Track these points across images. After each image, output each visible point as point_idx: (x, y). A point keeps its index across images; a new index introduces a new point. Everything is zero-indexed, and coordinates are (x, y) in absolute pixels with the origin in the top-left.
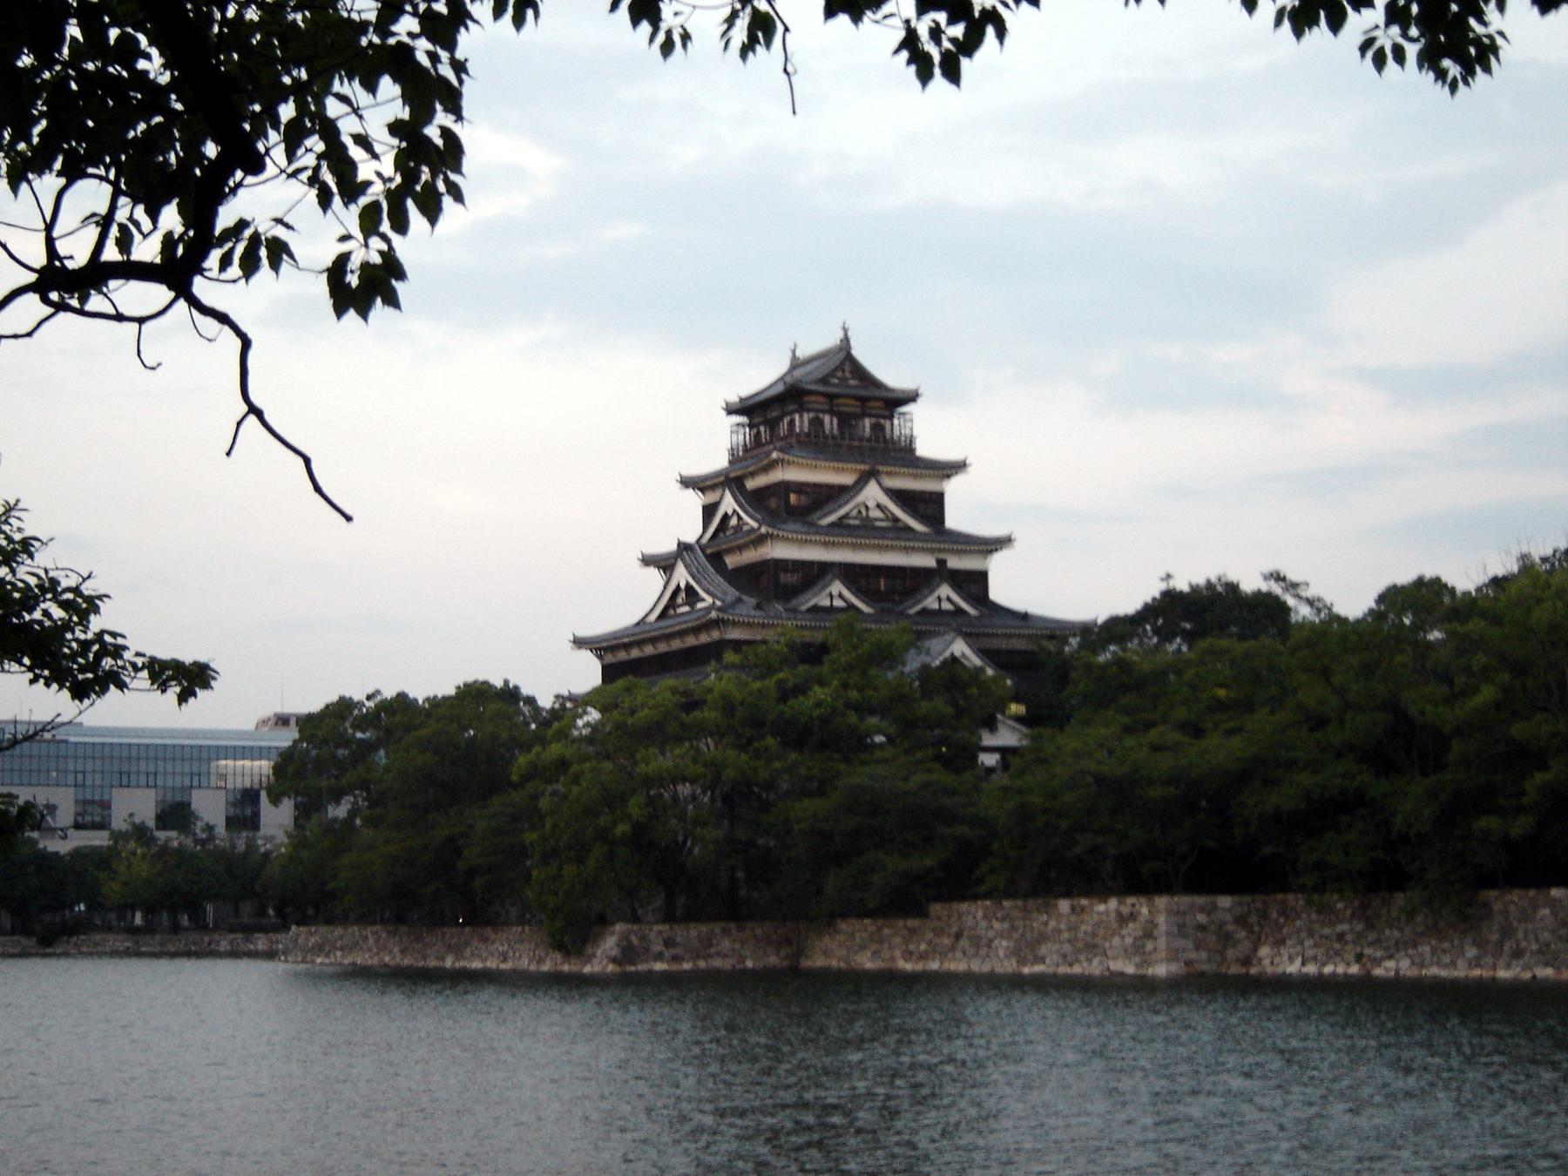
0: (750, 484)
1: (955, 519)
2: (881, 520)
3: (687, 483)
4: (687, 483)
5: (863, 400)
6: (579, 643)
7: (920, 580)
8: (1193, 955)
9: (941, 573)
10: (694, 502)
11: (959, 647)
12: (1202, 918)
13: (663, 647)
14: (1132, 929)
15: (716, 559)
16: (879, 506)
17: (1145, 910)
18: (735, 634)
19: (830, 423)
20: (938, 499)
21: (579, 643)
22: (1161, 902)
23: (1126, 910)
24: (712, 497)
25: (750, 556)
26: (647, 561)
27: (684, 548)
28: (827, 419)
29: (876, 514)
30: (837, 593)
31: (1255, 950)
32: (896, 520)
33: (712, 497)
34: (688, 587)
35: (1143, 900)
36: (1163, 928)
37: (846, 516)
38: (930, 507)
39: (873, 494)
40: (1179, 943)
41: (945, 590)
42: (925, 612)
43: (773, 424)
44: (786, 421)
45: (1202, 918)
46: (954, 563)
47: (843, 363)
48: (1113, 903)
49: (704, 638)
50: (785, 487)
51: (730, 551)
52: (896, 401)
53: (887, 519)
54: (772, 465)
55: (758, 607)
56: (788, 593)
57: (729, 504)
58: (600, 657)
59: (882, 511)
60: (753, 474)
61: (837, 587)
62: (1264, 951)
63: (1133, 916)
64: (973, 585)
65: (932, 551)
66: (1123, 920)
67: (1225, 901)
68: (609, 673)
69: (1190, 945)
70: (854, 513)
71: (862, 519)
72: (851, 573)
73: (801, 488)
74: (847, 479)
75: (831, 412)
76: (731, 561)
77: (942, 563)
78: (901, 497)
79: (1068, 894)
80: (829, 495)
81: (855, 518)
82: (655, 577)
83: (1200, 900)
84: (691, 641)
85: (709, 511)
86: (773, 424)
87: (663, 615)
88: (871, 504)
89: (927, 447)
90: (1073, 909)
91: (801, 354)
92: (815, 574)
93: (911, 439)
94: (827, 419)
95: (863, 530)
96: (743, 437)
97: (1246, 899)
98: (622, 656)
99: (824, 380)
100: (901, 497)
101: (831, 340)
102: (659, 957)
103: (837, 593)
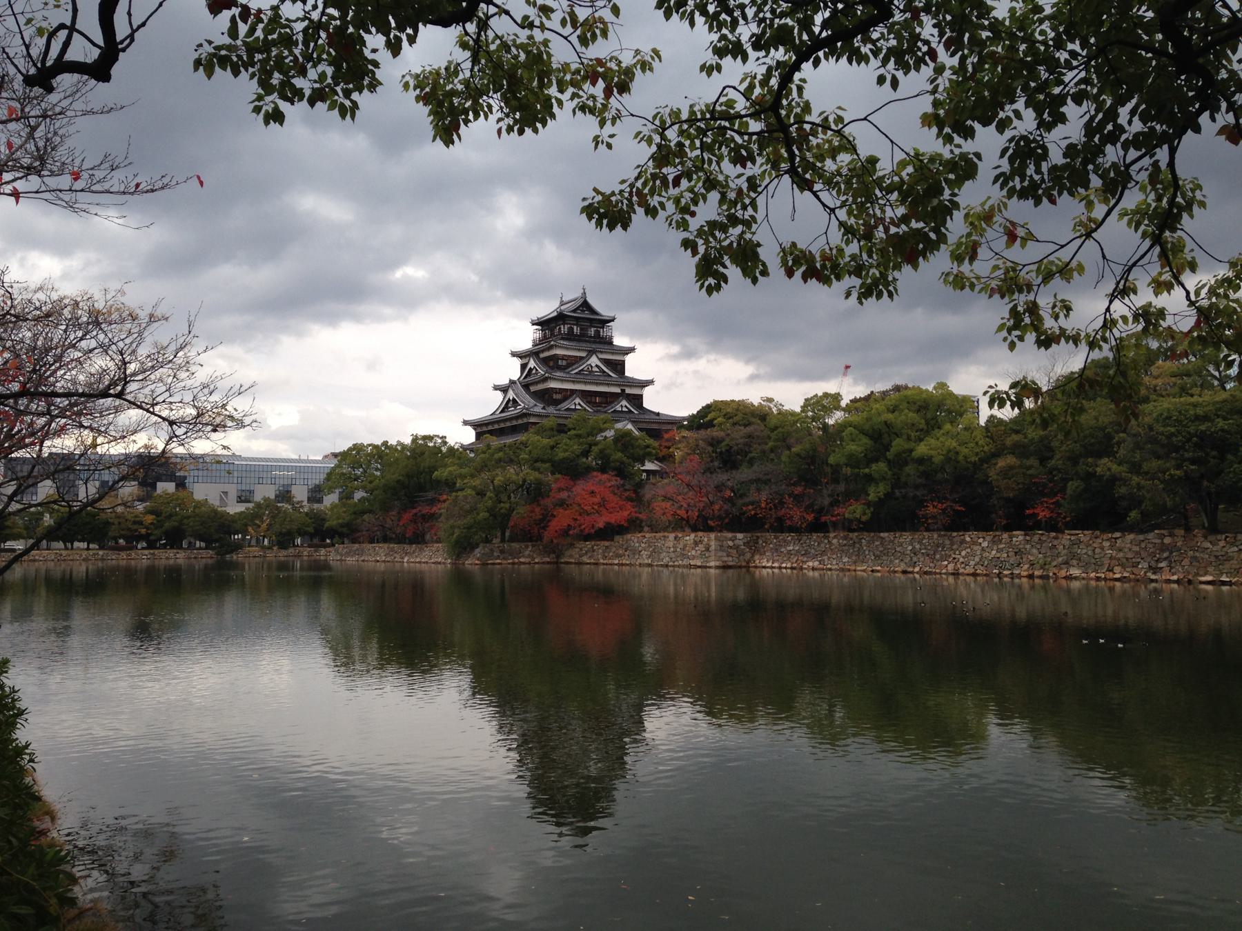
0: (542, 355)
1: (629, 373)
3: (514, 354)
4: (514, 354)
5: (591, 320)
6: (466, 423)
7: (614, 397)
8: (726, 559)
9: (623, 395)
10: (517, 362)
11: (630, 426)
12: (731, 543)
13: (502, 425)
14: (701, 547)
15: (526, 387)
16: (597, 366)
17: (706, 539)
18: (532, 420)
19: (576, 330)
20: (624, 362)
21: (466, 423)
22: (712, 536)
23: (698, 539)
24: (525, 361)
25: (541, 387)
26: (496, 388)
27: (512, 382)
31: (753, 556)
32: (604, 372)
33: (525, 361)
34: (514, 399)
35: (705, 534)
36: (713, 548)
37: (582, 370)
38: (619, 367)
39: (594, 361)
40: (720, 554)
41: (624, 403)
42: (615, 411)
43: (552, 331)
45: (731, 543)
46: (628, 391)
48: (693, 536)
49: (520, 422)
50: (555, 358)
51: (532, 384)
52: (604, 322)
54: (551, 348)
55: (544, 408)
56: (556, 403)
57: (532, 364)
58: (475, 429)
60: (543, 351)
61: (578, 401)
62: (757, 557)
63: (701, 542)
64: (637, 400)
65: (619, 385)
66: (696, 543)
67: (740, 536)
68: (478, 436)
69: (725, 554)
72: (585, 395)
73: (563, 357)
74: (583, 354)
75: (577, 325)
76: (533, 389)
77: (623, 391)
78: (607, 362)
79: (674, 530)
80: (578, 360)
82: (498, 397)
83: (730, 535)
84: (515, 423)
85: (523, 367)
86: (552, 331)
87: (502, 412)
88: (593, 365)
89: (620, 341)
90: (676, 538)
91: (565, 299)
93: (611, 338)
95: (587, 376)
96: (538, 335)
97: (749, 535)
98: (485, 429)
99: (574, 311)
100: (607, 362)
101: (577, 294)
102: (498, 558)
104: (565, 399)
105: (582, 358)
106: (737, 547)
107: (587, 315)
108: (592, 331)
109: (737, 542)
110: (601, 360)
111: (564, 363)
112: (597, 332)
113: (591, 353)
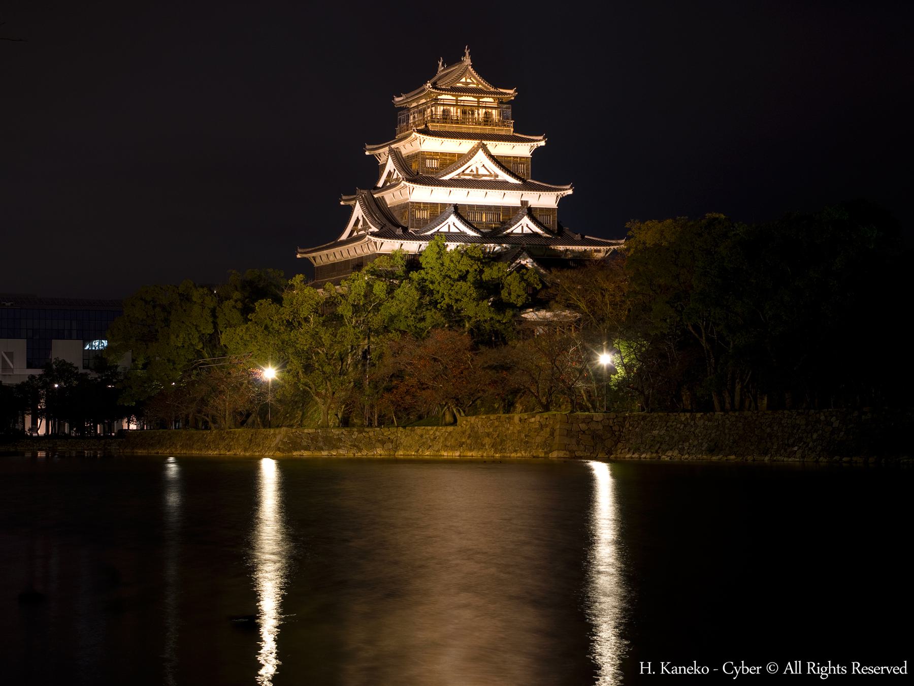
2: (486, 176)
29: (484, 172)
30: (453, 224)
32: (497, 176)
36: (557, 433)
44: (429, 110)
45: (583, 426)
50: (421, 157)
53: (491, 175)
59: (488, 171)
69: (574, 441)
70: (467, 172)
71: (474, 175)
80: (452, 161)
81: (469, 175)
90: (520, 420)
92: (438, 211)
103: (453, 224)
109: (593, 426)
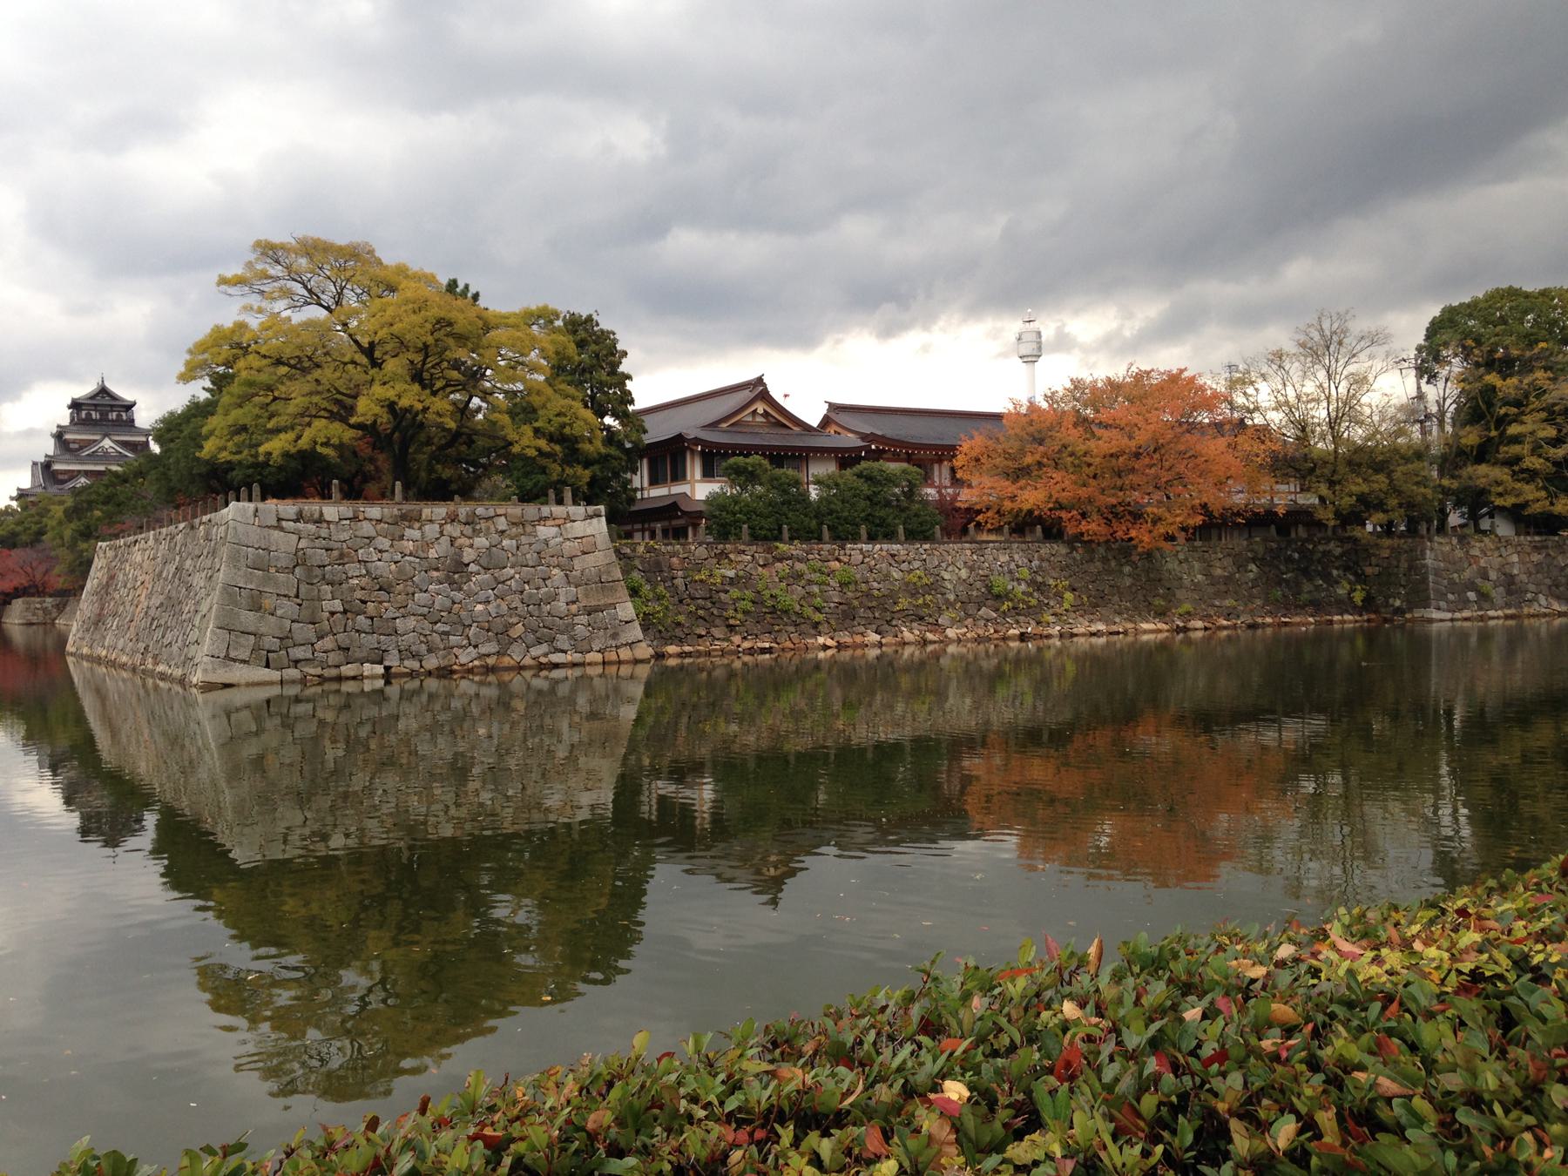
5: (112, 406)
28: (93, 413)
39: (107, 443)
45: (38, 606)
47: (103, 391)
56: (63, 482)
67: (49, 600)
73: (74, 441)
75: (96, 410)
78: (124, 444)
80: (85, 444)
92: (73, 475)
93: (133, 421)
94: (93, 413)
95: (105, 457)
100: (124, 444)
103: (83, 481)
104: (70, 479)
105: (95, 441)
106: (45, 610)
107: (107, 401)
108: (113, 416)
110: (114, 441)
111: (76, 446)
112: (119, 416)
113: (106, 435)
